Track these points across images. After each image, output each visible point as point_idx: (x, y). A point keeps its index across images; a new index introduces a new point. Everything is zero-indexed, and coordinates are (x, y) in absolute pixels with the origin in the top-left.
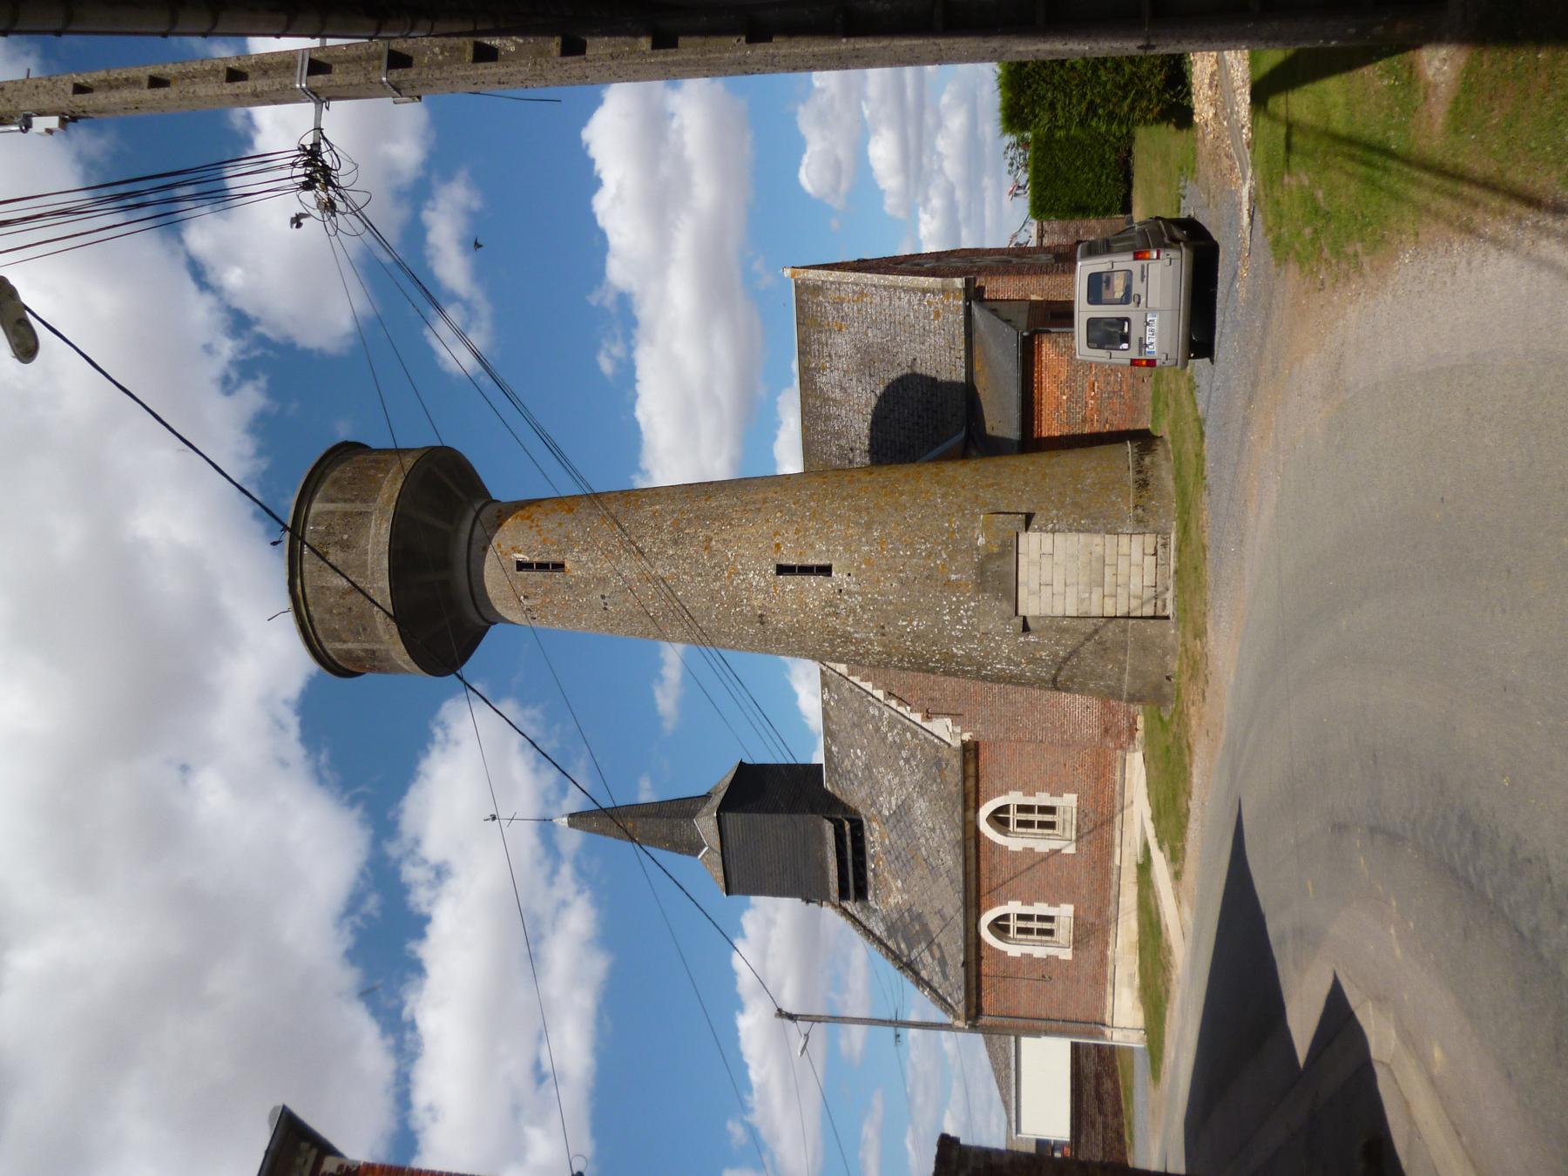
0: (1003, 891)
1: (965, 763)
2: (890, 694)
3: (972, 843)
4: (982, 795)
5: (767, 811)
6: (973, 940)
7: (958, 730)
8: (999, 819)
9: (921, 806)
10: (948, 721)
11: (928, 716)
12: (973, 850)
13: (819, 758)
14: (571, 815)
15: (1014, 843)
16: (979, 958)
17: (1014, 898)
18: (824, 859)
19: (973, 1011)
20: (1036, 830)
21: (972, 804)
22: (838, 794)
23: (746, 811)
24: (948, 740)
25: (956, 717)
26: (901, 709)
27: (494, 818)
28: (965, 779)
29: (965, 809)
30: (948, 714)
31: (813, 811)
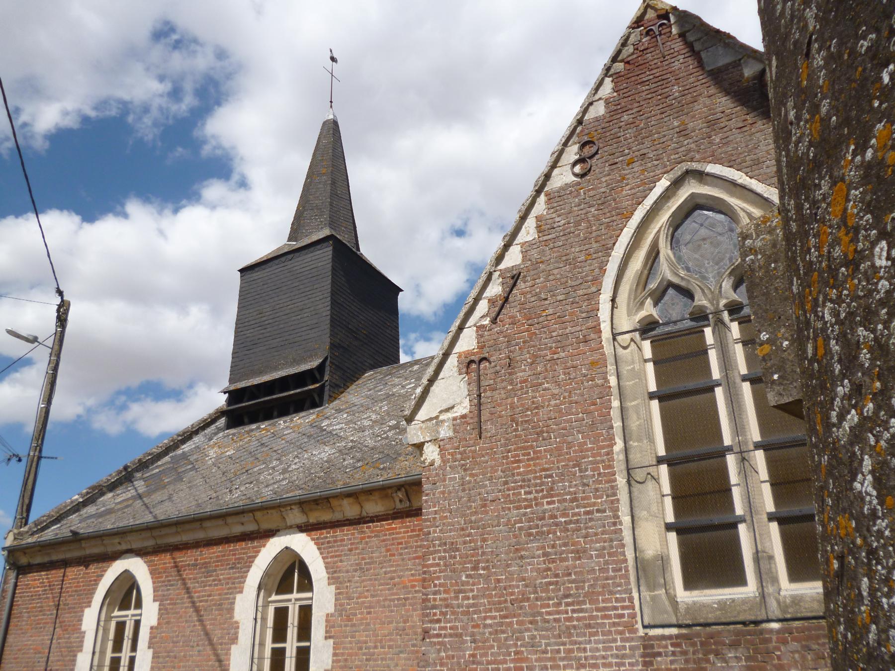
0: (176, 591)
1: (383, 491)
2: (514, 278)
3: (247, 525)
4: (328, 534)
5: (333, 293)
6: (114, 545)
7: (445, 432)
8: (291, 574)
9: (325, 453)
10: (464, 408)
11: (470, 364)
12: (237, 529)
13: (404, 358)
14: (335, 123)
15: (246, 605)
16: (85, 561)
17: (163, 612)
18: (276, 369)
19: (24, 560)
20: (269, 645)
21: (315, 517)
22: (360, 381)
23: (333, 269)
24: (422, 415)
25: (475, 422)
26: (483, 307)
27: (333, 59)
28: (354, 495)
29: (303, 504)
30: (478, 404)
31: (333, 346)
